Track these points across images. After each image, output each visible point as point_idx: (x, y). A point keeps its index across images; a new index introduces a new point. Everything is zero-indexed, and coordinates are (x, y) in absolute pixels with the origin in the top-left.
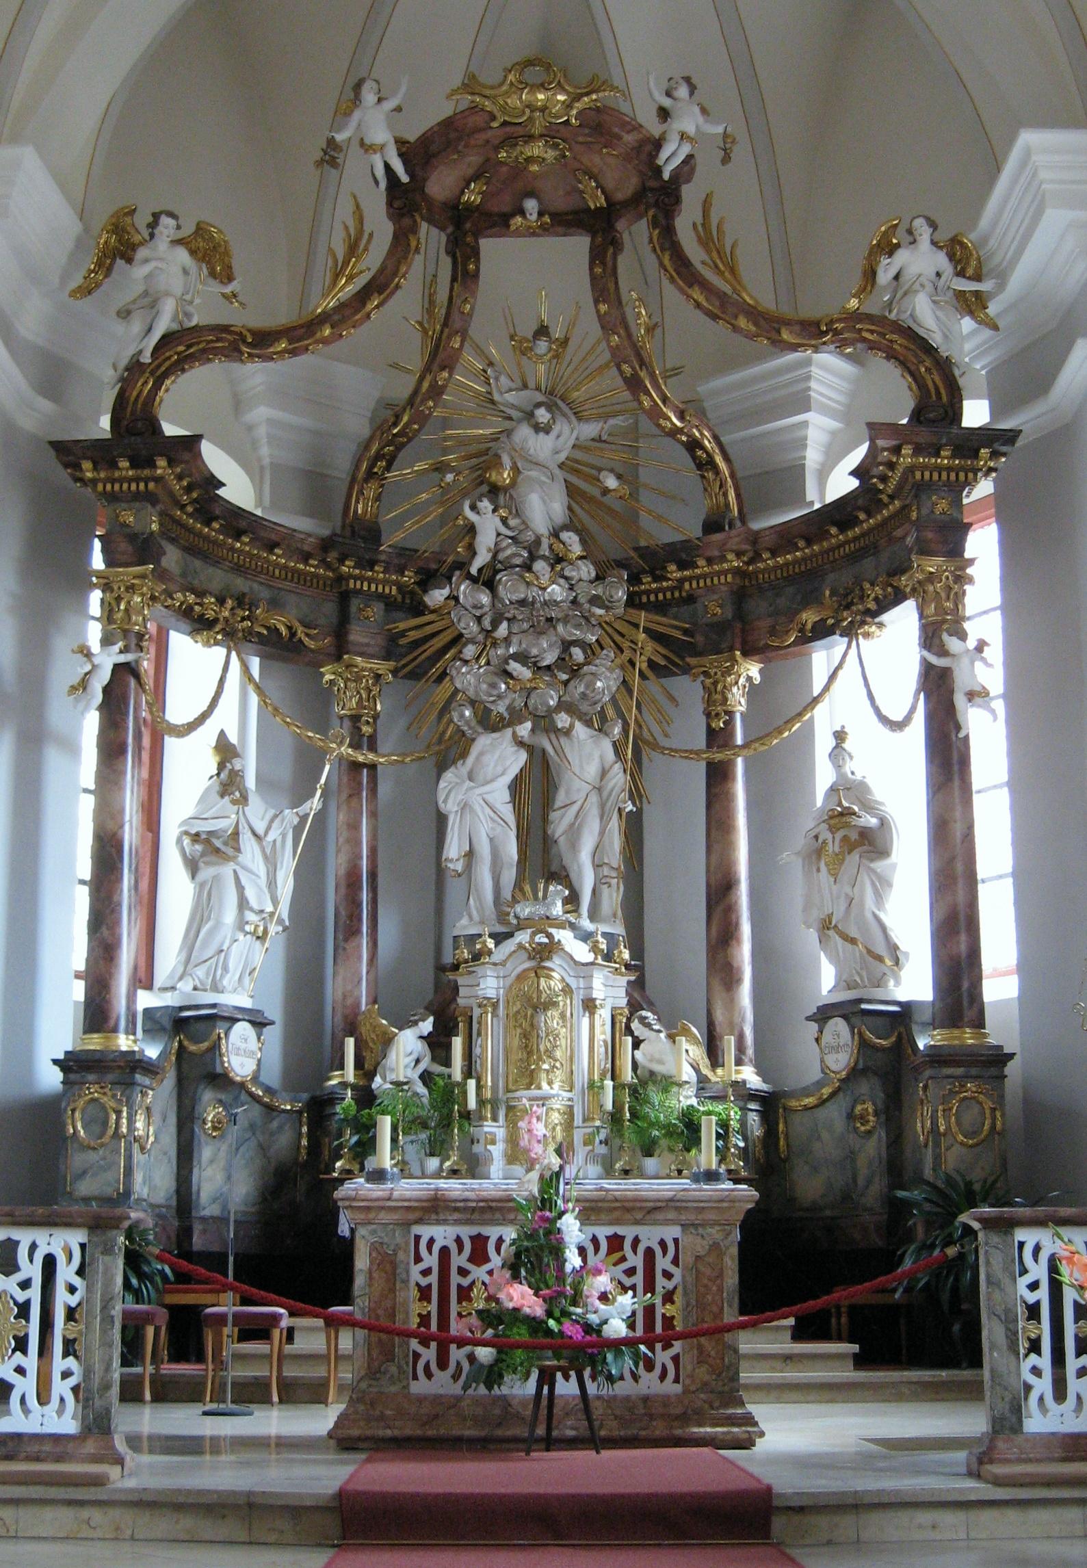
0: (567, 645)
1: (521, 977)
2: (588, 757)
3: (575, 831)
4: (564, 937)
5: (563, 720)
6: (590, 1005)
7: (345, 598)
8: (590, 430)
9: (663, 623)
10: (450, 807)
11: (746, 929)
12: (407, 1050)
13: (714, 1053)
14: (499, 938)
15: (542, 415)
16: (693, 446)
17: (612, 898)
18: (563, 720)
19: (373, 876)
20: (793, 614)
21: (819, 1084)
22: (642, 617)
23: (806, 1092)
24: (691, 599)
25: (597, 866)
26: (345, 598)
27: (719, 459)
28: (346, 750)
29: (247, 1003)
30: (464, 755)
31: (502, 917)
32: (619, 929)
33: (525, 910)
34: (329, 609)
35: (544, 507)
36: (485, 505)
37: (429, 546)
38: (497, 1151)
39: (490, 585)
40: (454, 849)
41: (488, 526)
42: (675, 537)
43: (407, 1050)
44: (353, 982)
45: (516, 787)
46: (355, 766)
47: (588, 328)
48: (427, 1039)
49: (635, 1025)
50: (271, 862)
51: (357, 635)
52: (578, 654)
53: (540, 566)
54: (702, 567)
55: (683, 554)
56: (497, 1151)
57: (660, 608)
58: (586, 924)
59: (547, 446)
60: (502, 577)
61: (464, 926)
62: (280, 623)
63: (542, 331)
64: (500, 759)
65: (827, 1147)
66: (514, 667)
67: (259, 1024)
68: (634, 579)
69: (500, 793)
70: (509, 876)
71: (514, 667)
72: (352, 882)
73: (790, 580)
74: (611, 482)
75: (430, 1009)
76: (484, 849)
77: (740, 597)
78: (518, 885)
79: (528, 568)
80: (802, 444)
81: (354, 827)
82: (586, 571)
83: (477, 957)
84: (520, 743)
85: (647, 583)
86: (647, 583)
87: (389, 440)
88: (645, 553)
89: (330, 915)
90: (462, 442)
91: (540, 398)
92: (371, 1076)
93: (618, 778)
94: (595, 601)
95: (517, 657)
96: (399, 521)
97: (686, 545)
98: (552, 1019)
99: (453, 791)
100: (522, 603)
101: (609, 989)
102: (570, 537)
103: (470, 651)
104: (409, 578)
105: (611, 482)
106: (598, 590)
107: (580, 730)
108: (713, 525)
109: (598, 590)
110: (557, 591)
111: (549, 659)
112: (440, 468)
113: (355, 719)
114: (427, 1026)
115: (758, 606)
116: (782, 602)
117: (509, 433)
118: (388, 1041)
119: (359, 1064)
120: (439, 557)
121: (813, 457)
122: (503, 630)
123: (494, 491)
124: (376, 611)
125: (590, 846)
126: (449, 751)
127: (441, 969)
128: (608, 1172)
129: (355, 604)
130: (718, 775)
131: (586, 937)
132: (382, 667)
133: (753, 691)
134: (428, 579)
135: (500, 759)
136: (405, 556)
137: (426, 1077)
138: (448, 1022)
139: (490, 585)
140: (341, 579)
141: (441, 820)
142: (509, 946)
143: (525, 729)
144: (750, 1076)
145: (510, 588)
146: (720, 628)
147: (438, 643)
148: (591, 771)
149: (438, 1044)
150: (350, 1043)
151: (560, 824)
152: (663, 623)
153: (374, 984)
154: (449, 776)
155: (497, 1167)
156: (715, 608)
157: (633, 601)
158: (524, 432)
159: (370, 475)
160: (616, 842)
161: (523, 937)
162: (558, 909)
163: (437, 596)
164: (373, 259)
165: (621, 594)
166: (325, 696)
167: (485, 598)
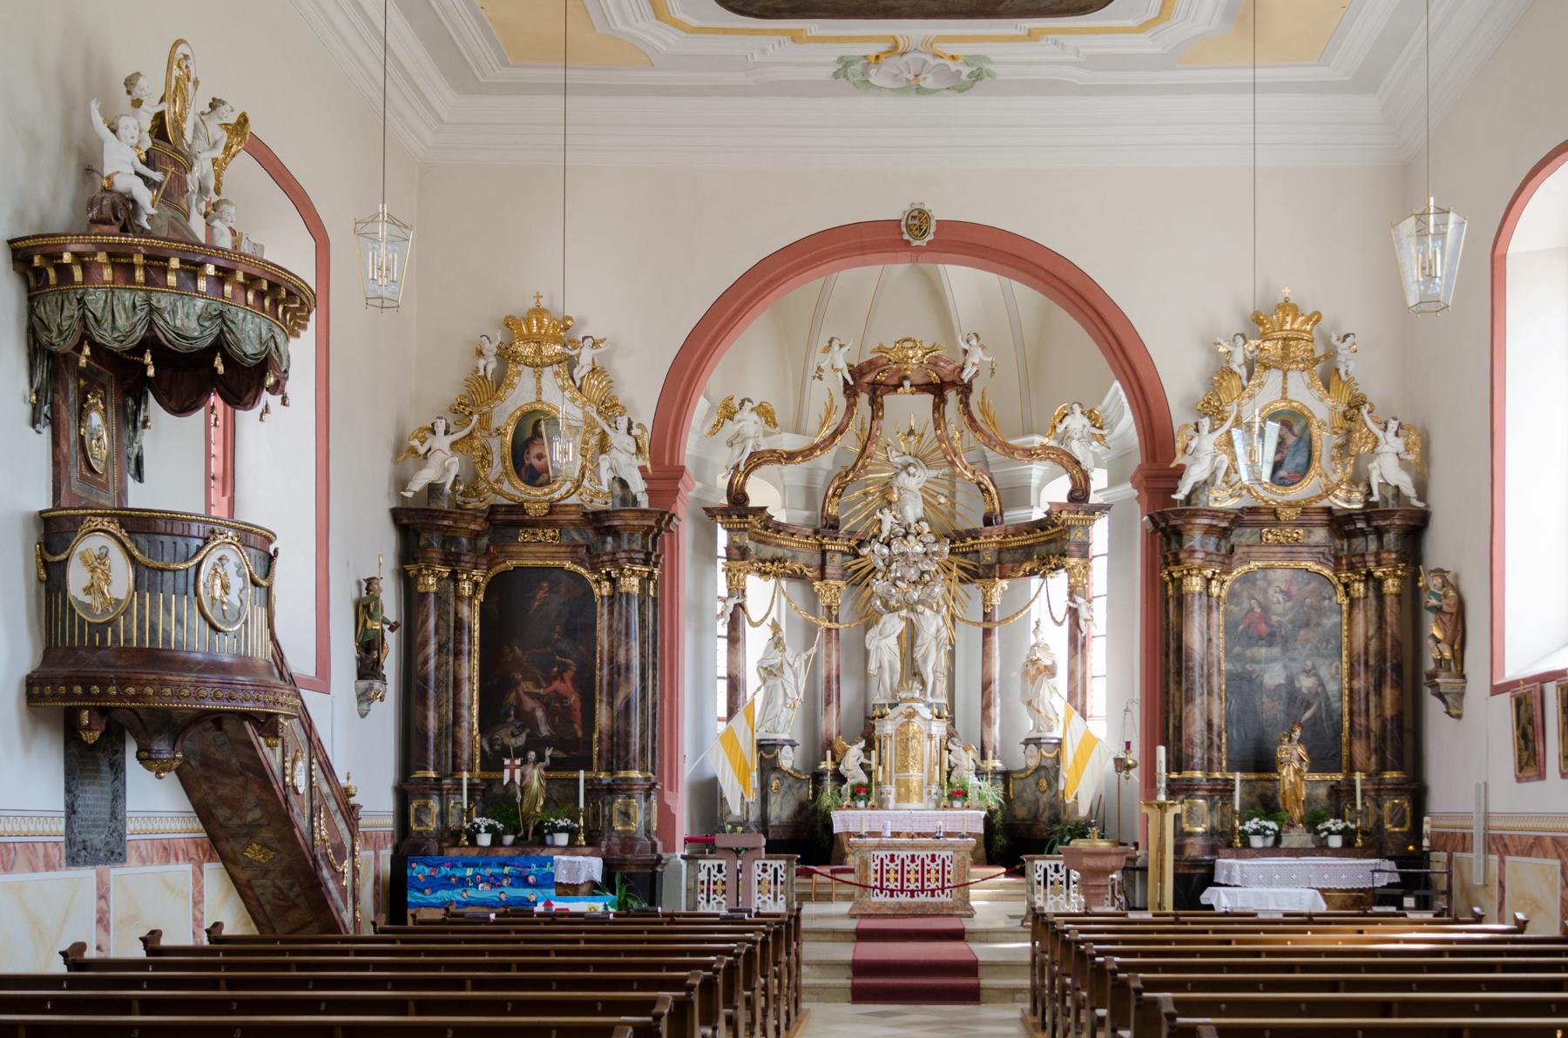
0: (923, 573)
1: (902, 725)
2: (932, 624)
3: (925, 658)
4: (919, 707)
5: (920, 608)
6: (930, 737)
7: (824, 553)
8: (932, 473)
9: (965, 562)
10: (871, 647)
11: (998, 701)
12: (854, 754)
13: (983, 756)
14: (892, 706)
15: (912, 470)
16: (979, 484)
17: (942, 686)
18: (920, 608)
19: (838, 677)
20: (1021, 563)
21: (1027, 768)
22: (956, 559)
23: (1021, 771)
24: (977, 552)
25: (935, 672)
26: (824, 553)
27: (992, 488)
28: (827, 624)
29: (786, 736)
30: (877, 622)
31: (894, 697)
32: (944, 701)
33: (903, 695)
34: (818, 557)
35: (913, 510)
36: (886, 511)
37: (860, 530)
38: (892, 798)
39: (888, 545)
40: (873, 666)
41: (888, 519)
42: (970, 527)
43: (854, 754)
44: (830, 723)
45: (899, 638)
46: (829, 630)
47: (930, 431)
48: (864, 750)
49: (951, 746)
50: (796, 676)
51: (829, 570)
52: (927, 577)
53: (910, 537)
54: (982, 539)
55: (974, 533)
56: (892, 798)
57: (964, 554)
58: (930, 700)
59: (913, 483)
60: (894, 542)
61: (877, 699)
62: (796, 567)
63: (911, 432)
64: (893, 625)
65: (1028, 795)
66: (899, 583)
67: (793, 745)
68: (953, 542)
69: (892, 641)
70: (897, 678)
71: (899, 583)
72: (828, 681)
73: (1021, 547)
74: (943, 500)
75: (863, 736)
76: (886, 666)
77: (1000, 552)
78: (901, 682)
79: (905, 537)
80: (1030, 477)
81: (829, 656)
82: (931, 538)
83: (882, 717)
84: (902, 618)
85: (958, 544)
86: (958, 544)
87: (844, 480)
88: (956, 532)
89: (821, 694)
90: (875, 482)
91: (911, 460)
92: (838, 764)
93: (944, 634)
94: (934, 553)
95: (902, 579)
96: (847, 520)
97: (975, 530)
98: (914, 743)
99: (872, 640)
100: (902, 554)
101: (939, 729)
102: (925, 525)
103: (879, 575)
104: (853, 543)
105: (943, 500)
106: (936, 548)
107: (928, 612)
108: (988, 521)
109: (936, 548)
110: (919, 549)
111: (915, 578)
112: (866, 494)
113: (829, 607)
114: (862, 744)
115: (1007, 557)
116: (1017, 556)
117: (897, 474)
118: (845, 750)
119: (833, 759)
120: (866, 532)
121: (1035, 482)
122: (894, 566)
123: (890, 503)
124: (838, 556)
125: (933, 662)
126: (869, 621)
127: (867, 718)
128: (938, 807)
129: (828, 555)
130: (987, 633)
131: (929, 706)
132: (841, 583)
133: (1004, 593)
134: (861, 543)
135: (893, 625)
136: (851, 533)
137: (862, 766)
138: (870, 742)
139: (888, 545)
140: (821, 545)
141: (866, 653)
142: (897, 710)
143: (904, 613)
144: (998, 764)
145: (896, 547)
146: (990, 567)
147: (865, 571)
148: (933, 630)
149: (867, 751)
150: (829, 753)
151: (918, 655)
152: (965, 562)
153: (839, 723)
154: (871, 633)
155: (892, 804)
156: (989, 558)
157: (952, 552)
158: (904, 475)
159: (834, 495)
160: (944, 661)
161: (902, 707)
162: (917, 694)
163: (865, 551)
164: (837, 418)
165: (947, 549)
166: (815, 596)
167: (885, 551)
